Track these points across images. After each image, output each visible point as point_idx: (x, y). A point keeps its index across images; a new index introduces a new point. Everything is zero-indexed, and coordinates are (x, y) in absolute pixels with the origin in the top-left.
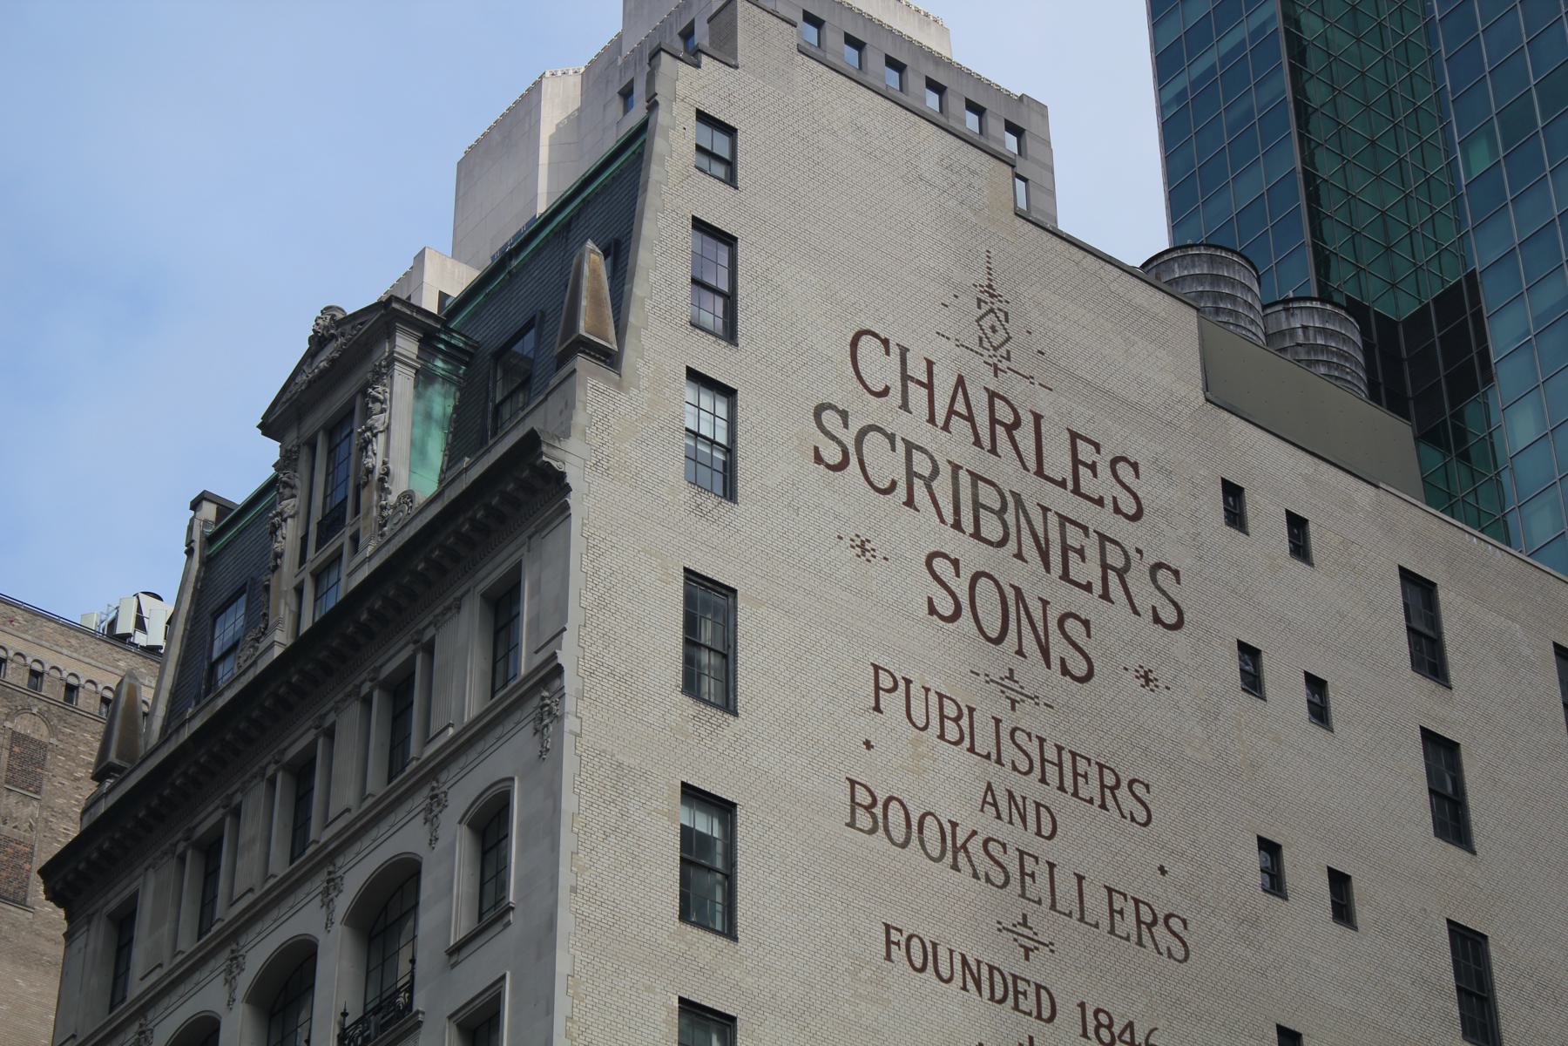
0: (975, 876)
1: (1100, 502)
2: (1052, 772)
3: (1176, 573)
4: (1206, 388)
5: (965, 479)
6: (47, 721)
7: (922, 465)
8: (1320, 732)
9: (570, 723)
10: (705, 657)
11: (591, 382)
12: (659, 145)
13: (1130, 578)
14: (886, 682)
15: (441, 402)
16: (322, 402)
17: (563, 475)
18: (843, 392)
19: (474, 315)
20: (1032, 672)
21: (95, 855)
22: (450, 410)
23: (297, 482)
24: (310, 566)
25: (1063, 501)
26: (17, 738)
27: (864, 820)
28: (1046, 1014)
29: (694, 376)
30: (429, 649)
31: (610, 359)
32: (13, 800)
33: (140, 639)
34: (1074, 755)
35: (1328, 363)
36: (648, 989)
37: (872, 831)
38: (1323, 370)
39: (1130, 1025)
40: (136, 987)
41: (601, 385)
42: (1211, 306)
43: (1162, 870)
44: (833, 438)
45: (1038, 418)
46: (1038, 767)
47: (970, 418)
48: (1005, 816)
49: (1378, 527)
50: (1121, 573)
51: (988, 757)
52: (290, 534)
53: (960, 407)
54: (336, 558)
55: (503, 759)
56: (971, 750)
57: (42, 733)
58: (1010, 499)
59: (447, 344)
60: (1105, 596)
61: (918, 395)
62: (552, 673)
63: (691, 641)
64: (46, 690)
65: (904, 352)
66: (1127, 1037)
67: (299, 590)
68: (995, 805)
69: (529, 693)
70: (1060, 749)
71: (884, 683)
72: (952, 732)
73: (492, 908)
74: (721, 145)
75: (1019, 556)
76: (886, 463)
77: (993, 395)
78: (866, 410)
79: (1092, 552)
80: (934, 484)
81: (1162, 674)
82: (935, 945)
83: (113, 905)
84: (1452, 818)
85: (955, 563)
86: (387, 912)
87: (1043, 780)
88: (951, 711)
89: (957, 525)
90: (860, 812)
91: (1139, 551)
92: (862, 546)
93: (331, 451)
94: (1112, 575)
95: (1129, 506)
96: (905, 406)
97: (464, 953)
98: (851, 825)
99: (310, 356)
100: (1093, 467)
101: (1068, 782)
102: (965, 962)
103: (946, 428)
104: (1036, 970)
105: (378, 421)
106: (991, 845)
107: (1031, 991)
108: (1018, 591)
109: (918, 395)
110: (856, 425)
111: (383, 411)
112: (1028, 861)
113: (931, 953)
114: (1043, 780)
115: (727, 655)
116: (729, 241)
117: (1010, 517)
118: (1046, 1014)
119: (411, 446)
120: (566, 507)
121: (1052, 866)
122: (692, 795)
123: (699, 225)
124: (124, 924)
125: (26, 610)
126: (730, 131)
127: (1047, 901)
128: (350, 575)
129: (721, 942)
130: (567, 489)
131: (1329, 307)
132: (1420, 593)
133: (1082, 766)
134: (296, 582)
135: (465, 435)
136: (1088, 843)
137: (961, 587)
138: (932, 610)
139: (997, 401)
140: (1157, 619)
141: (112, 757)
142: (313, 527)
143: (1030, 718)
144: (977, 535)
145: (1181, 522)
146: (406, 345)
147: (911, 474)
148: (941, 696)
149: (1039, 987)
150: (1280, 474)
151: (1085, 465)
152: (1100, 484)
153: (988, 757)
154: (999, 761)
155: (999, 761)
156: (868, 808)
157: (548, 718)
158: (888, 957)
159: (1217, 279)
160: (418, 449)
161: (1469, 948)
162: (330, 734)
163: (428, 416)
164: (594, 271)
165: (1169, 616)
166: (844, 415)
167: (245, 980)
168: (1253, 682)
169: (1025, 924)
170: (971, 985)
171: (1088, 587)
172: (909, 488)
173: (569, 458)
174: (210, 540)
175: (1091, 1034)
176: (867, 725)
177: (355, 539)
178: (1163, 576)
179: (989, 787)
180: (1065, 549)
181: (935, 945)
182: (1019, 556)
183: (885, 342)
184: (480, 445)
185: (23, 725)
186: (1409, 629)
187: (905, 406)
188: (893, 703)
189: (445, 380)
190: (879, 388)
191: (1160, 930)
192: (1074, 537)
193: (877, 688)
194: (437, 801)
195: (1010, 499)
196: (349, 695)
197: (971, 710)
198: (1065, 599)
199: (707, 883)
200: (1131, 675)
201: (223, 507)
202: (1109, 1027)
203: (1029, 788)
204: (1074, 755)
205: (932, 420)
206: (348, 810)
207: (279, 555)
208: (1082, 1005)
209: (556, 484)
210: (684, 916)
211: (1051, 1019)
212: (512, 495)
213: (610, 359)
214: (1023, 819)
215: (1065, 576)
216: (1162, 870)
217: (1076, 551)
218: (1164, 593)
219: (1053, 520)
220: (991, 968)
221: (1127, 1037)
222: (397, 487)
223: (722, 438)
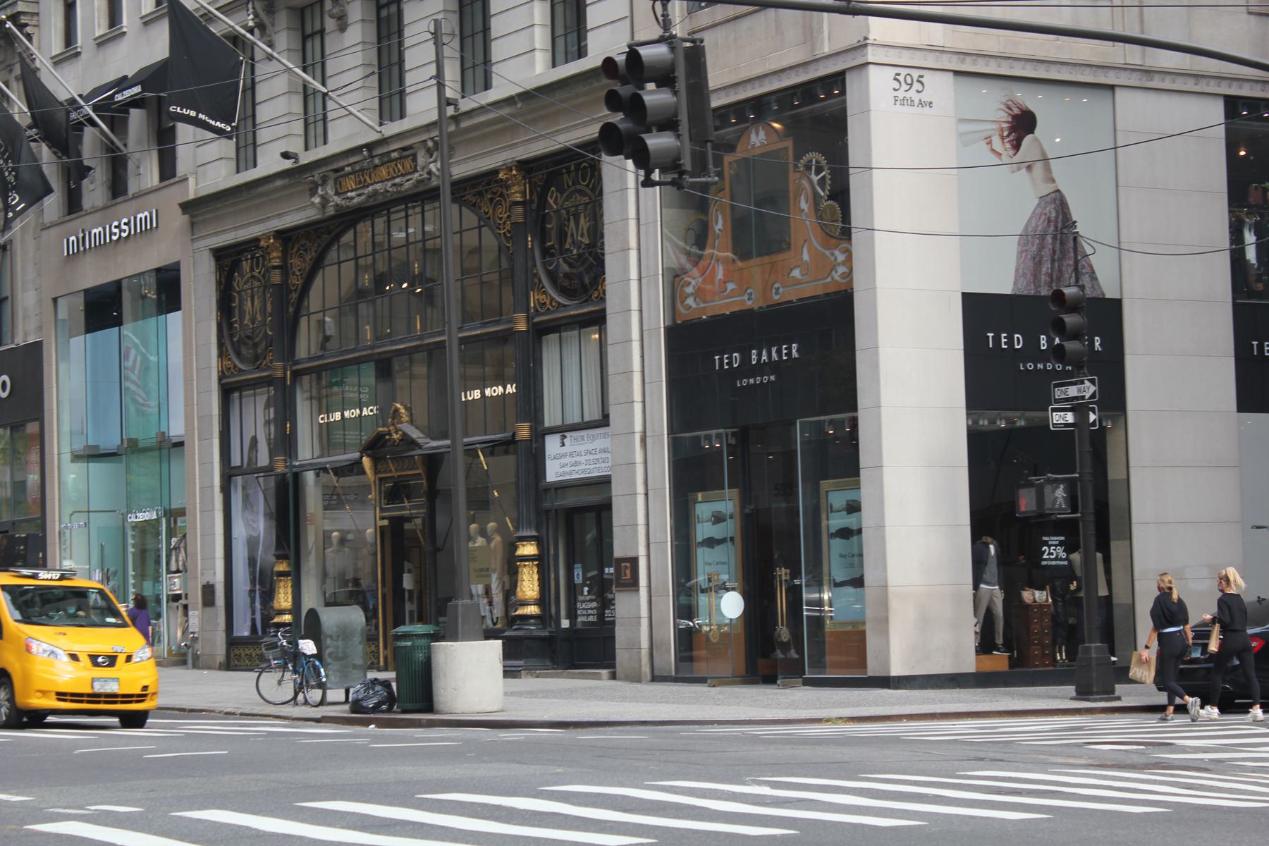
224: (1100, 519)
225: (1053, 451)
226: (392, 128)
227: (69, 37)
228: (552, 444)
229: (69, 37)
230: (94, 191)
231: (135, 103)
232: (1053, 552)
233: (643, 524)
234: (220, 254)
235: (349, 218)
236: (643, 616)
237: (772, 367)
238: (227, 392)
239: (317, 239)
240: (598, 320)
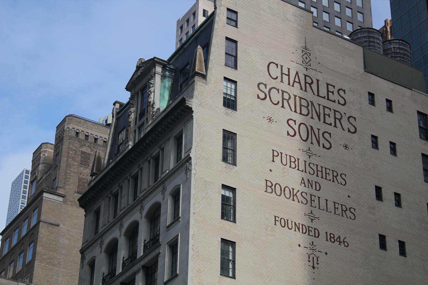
0: (299, 202)
1: (334, 101)
2: (320, 173)
3: (355, 118)
4: (365, 68)
5: (298, 99)
6: (90, 148)
7: (286, 96)
8: (393, 157)
9: (193, 172)
10: (229, 151)
11: (199, 83)
12: (217, 19)
13: (342, 121)
14: (276, 154)
15: (168, 83)
16: (140, 81)
17: (191, 108)
18: (265, 79)
19: (176, 59)
20: (315, 148)
21: (90, 197)
22: (170, 85)
23: (134, 103)
24: (137, 125)
26: (83, 153)
27: (269, 190)
28: (317, 236)
29: (225, 79)
30: (163, 150)
32: (82, 168)
34: (326, 168)
35: (400, 57)
36: (213, 237)
37: (272, 193)
38: (399, 59)
39: (339, 237)
40: (100, 230)
41: (201, 84)
43: (349, 197)
44: (263, 91)
45: (318, 81)
46: (316, 172)
47: (299, 83)
48: (307, 186)
50: (340, 120)
51: (303, 171)
52: (133, 116)
53: (297, 80)
54: (143, 124)
56: (298, 169)
58: (310, 103)
59: (169, 68)
60: (335, 126)
61: (285, 78)
63: (225, 148)
64: (89, 140)
65: (282, 67)
66: (338, 240)
67: (135, 131)
68: (304, 183)
69: (184, 163)
70: (322, 167)
71: (275, 154)
72: (293, 165)
73: (176, 217)
74: (233, 17)
75: (312, 118)
76: (276, 96)
77: (306, 76)
78: (271, 83)
79: (332, 115)
80: (289, 101)
81: (350, 145)
82: (287, 220)
83: (95, 208)
85: (295, 121)
86: (154, 216)
87: (317, 176)
88: (293, 160)
89: (295, 111)
90: (268, 188)
91: (345, 113)
92: (270, 119)
93: (142, 95)
94: (337, 121)
95: (342, 102)
96: (282, 81)
97: (170, 228)
98: (266, 191)
99: (136, 71)
100: (333, 92)
101: (324, 176)
102: (295, 224)
103: (293, 86)
104: (314, 225)
105: (152, 89)
106: (303, 194)
107: (313, 230)
108: (312, 127)
109: (285, 78)
110: (268, 88)
111: (153, 87)
112: (313, 197)
113: (286, 222)
114: (317, 176)
115: (234, 151)
116: (235, 42)
117: (310, 108)
118: (317, 236)
120: (192, 116)
121: (319, 198)
122: (224, 187)
123: (227, 38)
124: (97, 213)
125: (84, 120)
126: (236, 13)
127: (318, 207)
128: (146, 129)
129: (232, 224)
130: (193, 112)
131: (401, 42)
133: (328, 171)
134: (134, 129)
136: (329, 191)
137: (296, 128)
138: (288, 134)
139: (307, 77)
140: (349, 131)
141: (94, 171)
142: (138, 115)
143: (314, 160)
144: (301, 113)
145: (356, 104)
146: (159, 69)
147: (283, 99)
148: (290, 156)
149: (315, 229)
150: (384, 88)
151: (331, 92)
152: (335, 97)
153: (303, 171)
154: (305, 172)
155: (305, 172)
156: (270, 187)
157: (188, 170)
158: (275, 224)
159: (369, 37)
160: (162, 96)
162: (141, 169)
163: (165, 87)
164: (200, 54)
165: (352, 130)
166: (265, 85)
167: (124, 230)
169: (312, 213)
170: (297, 230)
171: (331, 124)
173: (193, 104)
174: (118, 113)
175: (329, 240)
176: (271, 165)
177: (147, 119)
178: (351, 120)
179: (303, 179)
180: (325, 115)
181: (287, 220)
182: (312, 118)
183: (277, 65)
185: (84, 149)
186: (419, 127)
187: (282, 81)
189: (169, 77)
190: (275, 77)
191: (348, 212)
192: (327, 111)
193: (273, 156)
194: (164, 189)
195: (310, 103)
196: (146, 160)
197: (298, 159)
198: (324, 128)
199: (228, 209)
200: (342, 146)
201: (121, 105)
202: (334, 238)
203: (314, 178)
204: (326, 168)
205: (289, 84)
206: (145, 189)
207: (130, 122)
208: (326, 233)
209: (190, 110)
210: (222, 218)
211: (318, 237)
212: (180, 113)
213: (204, 77)
214: (312, 186)
215: (324, 122)
216: (349, 197)
217: (328, 115)
218: (351, 124)
219: (321, 107)
220: (302, 225)
221: (338, 240)
222: (156, 107)
223: (233, 94)
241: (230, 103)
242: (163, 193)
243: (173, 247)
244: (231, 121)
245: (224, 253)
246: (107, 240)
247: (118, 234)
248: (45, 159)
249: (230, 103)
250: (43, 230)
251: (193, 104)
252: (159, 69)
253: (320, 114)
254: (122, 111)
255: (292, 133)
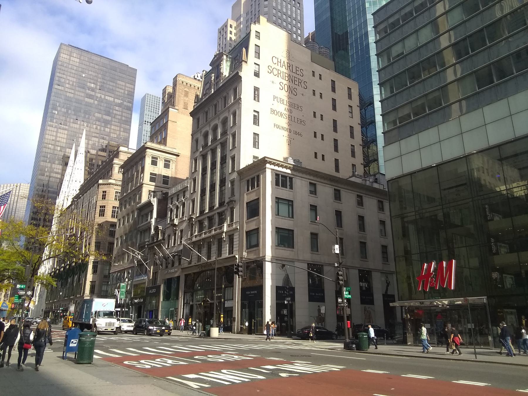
7: (279, 72)
15: (229, 64)
25: (295, 75)
31: (246, 62)
33: (198, 79)
40: (200, 127)
42: (312, 49)
49: (329, 75)
55: (235, 108)
57: (188, 90)
61: (279, 63)
62: (240, 99)
63: (255, 94)
69: (238, 101)
71: (275, 97)
74: (258, 34)
76: (276, 72)
78: (274, 66)
84: (334, 108)
86: (225, 122)
99: (214, 58)
109: (279, 63)
115: (258, 95)
119: (225, 70)
122: (255, 111)
124: (198, 119)
132: (333, 82)
135: (231, 69)
136: (296, 114)
146: (225, 57)
150: (318, 69)
160: (226, 69)
161: (335, 122)
167: (211, 127)
168: (314, 94)
172: (278, 75)
184: (233, 72)
185: (186, 89)
188: (276, 100)
194: (229, 111)
199: (256, 120)
213: (246, 62)
222: (224, 74)
224: (292, 314)
225: (285, 306)
226: (209, 261)
227: (168, 246)
228: (226, 302)
229: (168, 246)
230: (170, 266)
231: (177, 255)
232: (286, 319)
233: (237, 313)
234: (185, 275)
235: (203, 271)
236: (236, 325)
237: (253, 294)
238: (185, 293)
239: (198, 274)
240: (233, 286)
241: (257, 74)
242: (229, 113)
243: (234, 136)
244: (257, 82)
245: (254, 138)
246: (204, 131)
247: (209, 129)
248: (169, 93)
249: (257, 74)
250: (170, 124)
251: (241, 74)
252: (225, 57)
253: (295, 81)
254: (207, 75)
255: (281, 88)
